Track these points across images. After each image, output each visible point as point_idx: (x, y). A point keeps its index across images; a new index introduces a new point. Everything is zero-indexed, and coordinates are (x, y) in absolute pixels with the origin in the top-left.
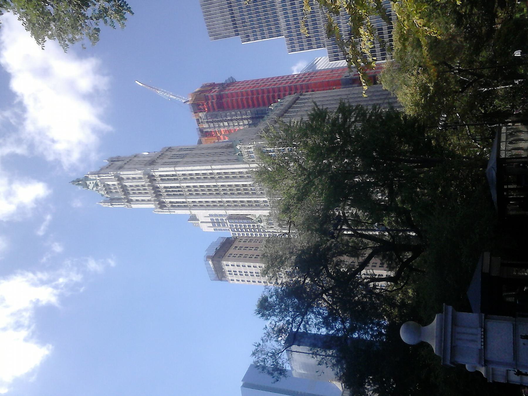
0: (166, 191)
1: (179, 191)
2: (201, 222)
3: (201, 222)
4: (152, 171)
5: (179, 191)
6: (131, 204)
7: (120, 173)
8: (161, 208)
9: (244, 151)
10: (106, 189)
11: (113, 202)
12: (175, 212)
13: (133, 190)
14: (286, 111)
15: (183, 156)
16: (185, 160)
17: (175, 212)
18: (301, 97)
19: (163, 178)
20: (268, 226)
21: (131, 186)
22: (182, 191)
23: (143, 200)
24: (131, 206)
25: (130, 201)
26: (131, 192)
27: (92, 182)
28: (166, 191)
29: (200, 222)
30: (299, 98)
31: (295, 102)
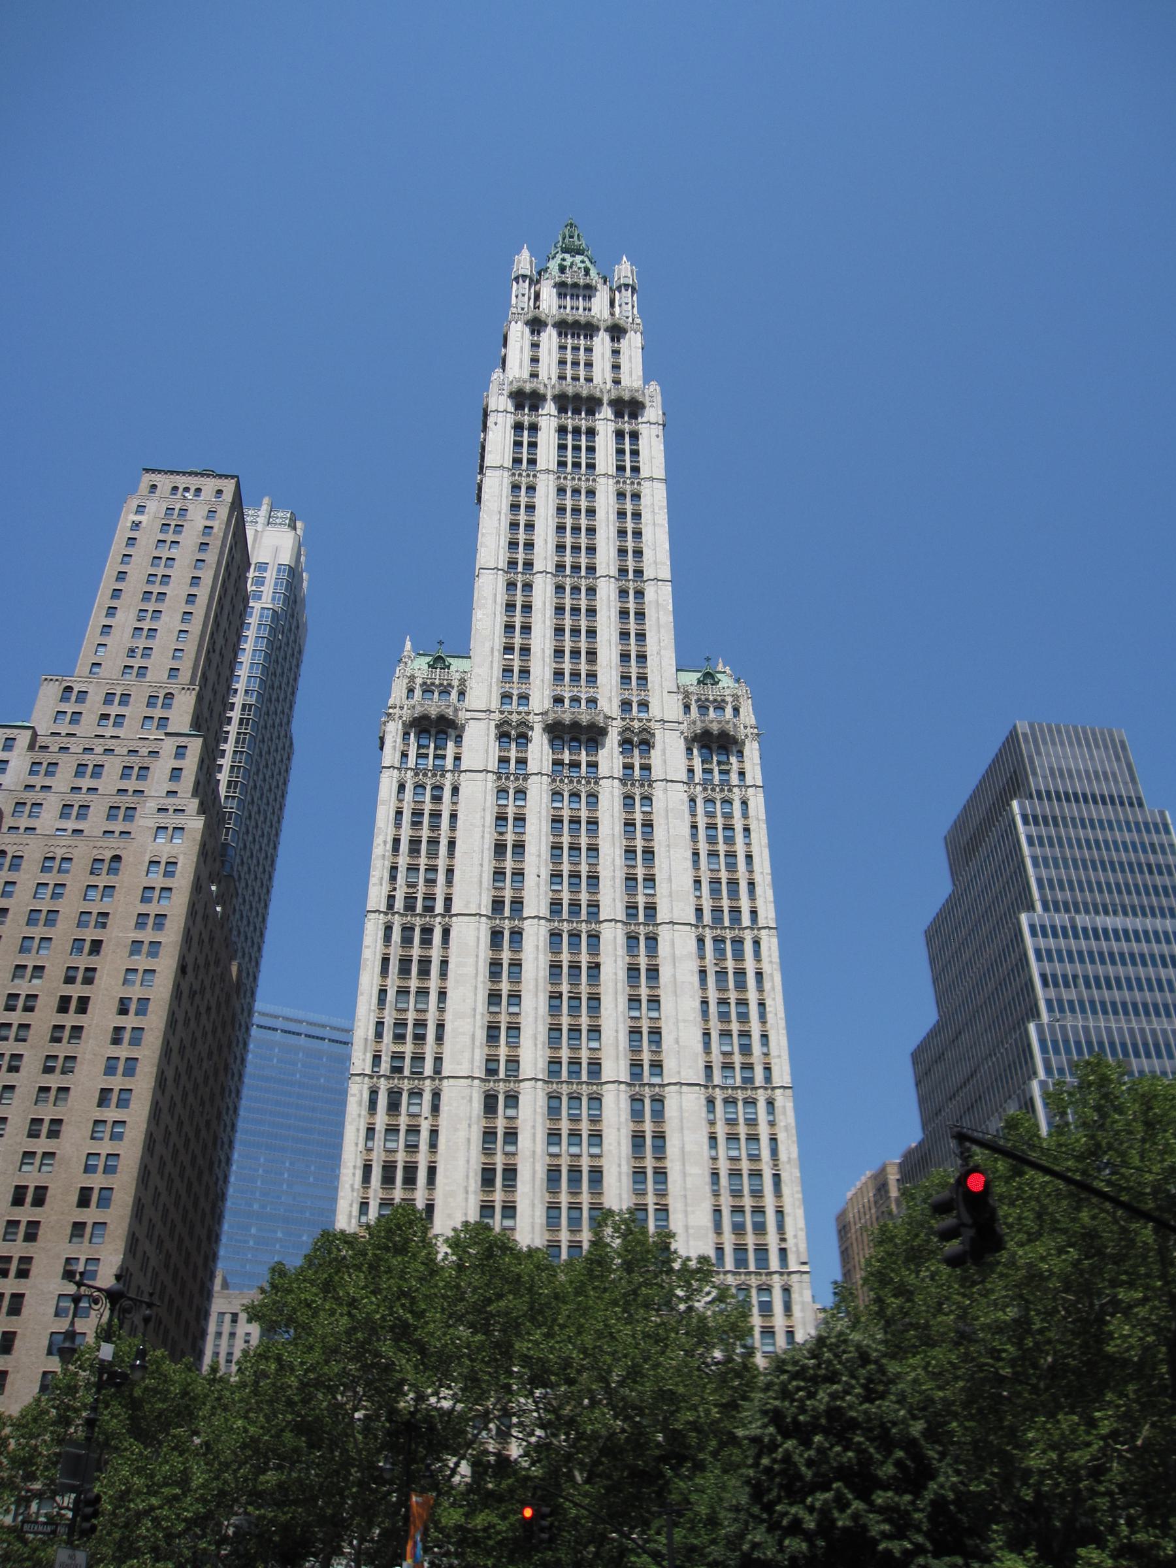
1: (577, 465)
5: (577, 465)
13: (576, 349)
19: (627, 441)
20: (419, 681)
21: (589, 350)
28: (577, 431)
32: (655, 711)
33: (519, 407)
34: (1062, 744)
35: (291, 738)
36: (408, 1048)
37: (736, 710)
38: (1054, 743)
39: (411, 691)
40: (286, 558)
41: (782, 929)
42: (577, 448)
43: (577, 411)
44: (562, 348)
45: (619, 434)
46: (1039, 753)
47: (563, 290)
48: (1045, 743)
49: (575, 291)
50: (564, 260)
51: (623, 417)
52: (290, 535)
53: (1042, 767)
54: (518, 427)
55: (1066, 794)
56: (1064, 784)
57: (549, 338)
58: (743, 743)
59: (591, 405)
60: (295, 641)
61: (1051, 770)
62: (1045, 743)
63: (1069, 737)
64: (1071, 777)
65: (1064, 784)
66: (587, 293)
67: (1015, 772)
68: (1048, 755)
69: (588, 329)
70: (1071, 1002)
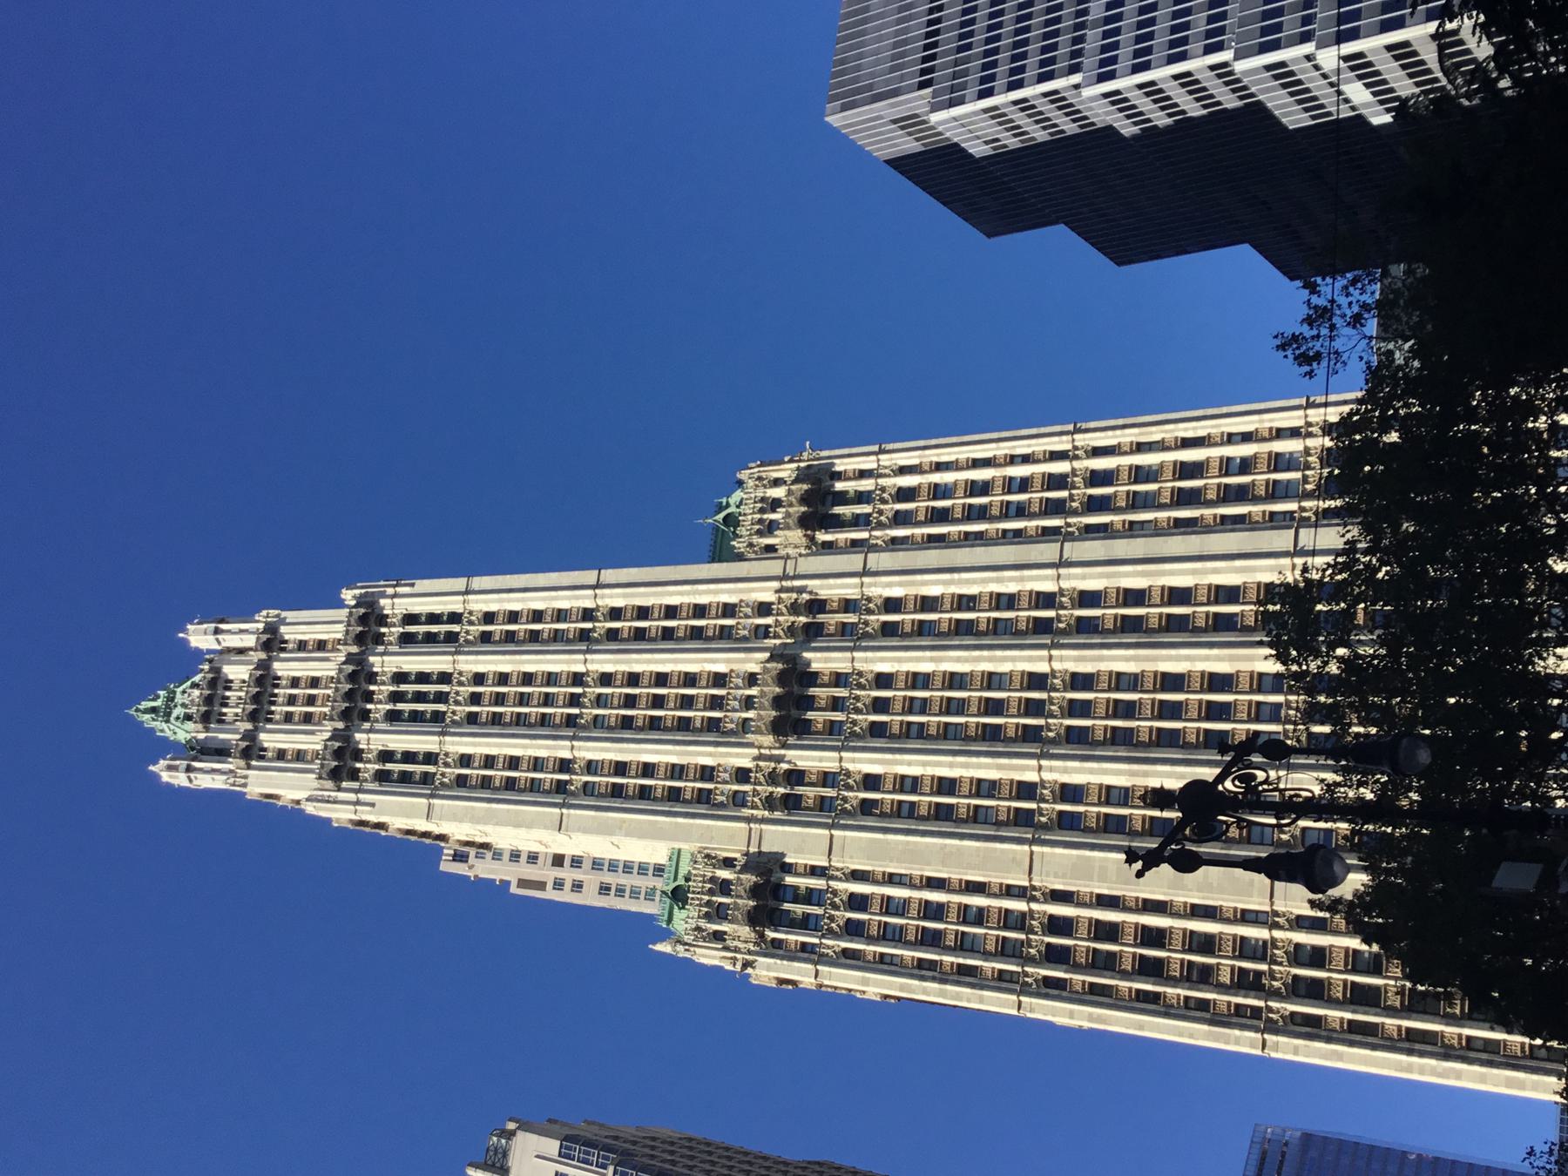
1: (441, 698)
4: (390, 591)
5: (441, 698)
6: (249, 767)
7: (285, 618)
8: (336, 775)
11: (200, 761)
12: (372, 805)
13: (292, 700)
17: (372, 805)
20: (703, 924)
21: (295, 682)
23: (299, 756)
24: (245, 777)
25: (251, 752)
26: (279, 709)
28: (396, 697)
32: (765, 593)
33: (354, 775)
34: (860, 56)
35: (809, 1162)
36: (1226, 965)
37: (777, 482)
38: (858, 68)
39: (718, 936)
40: (552, 1146)
41: (1076, 415)
42: (420, 697)
43: (369, 697)
44: (288, 718)
45: (407, 639)
46: (870, 87)
47: (214, 717)
48: (855, 79)
49: (217, 701)
50: (178, 718)
51: (384, 634)
52: (520, 1134)
53: (887, 83)
54: (382, 777)
55: (927, 47)
56: (914, 52)
57: (270, 740)
59: (359, 676)
60: (672, 1144)
61: (893, 69)
62: (855, 79)
63: (852, 48)
64: (905, 42)
65: (914, 52)
66: (220, 685)
67: (894, 122)
68: (873, 75)
69: (265, 680)
70: (1211, 20)
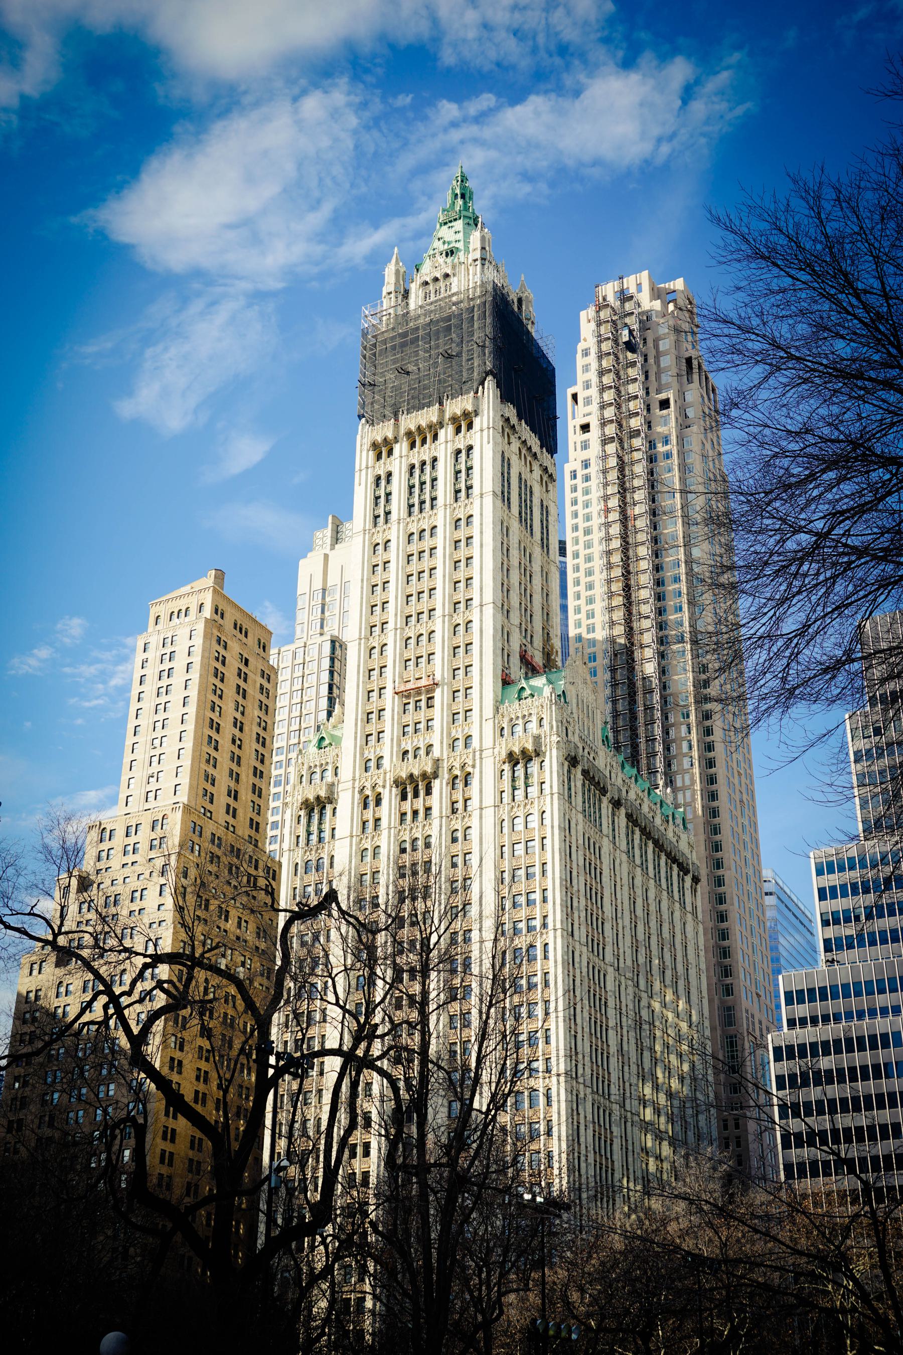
0: (423, 463)
1: (422, 502)
2: (326, 556)
3: (326, 556)
9: (531, 706)
10: (436, 279)
14: (647, 833)
15: (525, 519)
16: (515, 525)
18: (688, 879)
20: (306, 767)
22: (421, 511)
27: (460, 236)
29: (327, 551)
30: (686, 872)
31: (675, 860)
33: (379, 457)
42: (423, 483)
58: (545, 753)
